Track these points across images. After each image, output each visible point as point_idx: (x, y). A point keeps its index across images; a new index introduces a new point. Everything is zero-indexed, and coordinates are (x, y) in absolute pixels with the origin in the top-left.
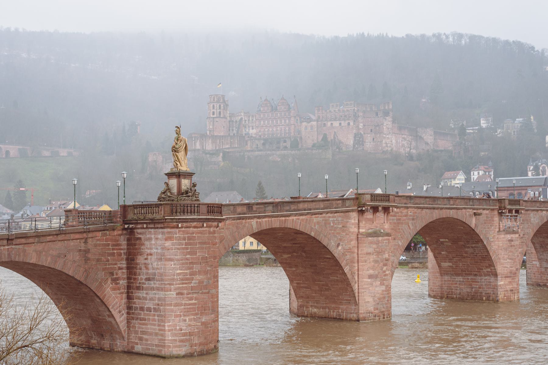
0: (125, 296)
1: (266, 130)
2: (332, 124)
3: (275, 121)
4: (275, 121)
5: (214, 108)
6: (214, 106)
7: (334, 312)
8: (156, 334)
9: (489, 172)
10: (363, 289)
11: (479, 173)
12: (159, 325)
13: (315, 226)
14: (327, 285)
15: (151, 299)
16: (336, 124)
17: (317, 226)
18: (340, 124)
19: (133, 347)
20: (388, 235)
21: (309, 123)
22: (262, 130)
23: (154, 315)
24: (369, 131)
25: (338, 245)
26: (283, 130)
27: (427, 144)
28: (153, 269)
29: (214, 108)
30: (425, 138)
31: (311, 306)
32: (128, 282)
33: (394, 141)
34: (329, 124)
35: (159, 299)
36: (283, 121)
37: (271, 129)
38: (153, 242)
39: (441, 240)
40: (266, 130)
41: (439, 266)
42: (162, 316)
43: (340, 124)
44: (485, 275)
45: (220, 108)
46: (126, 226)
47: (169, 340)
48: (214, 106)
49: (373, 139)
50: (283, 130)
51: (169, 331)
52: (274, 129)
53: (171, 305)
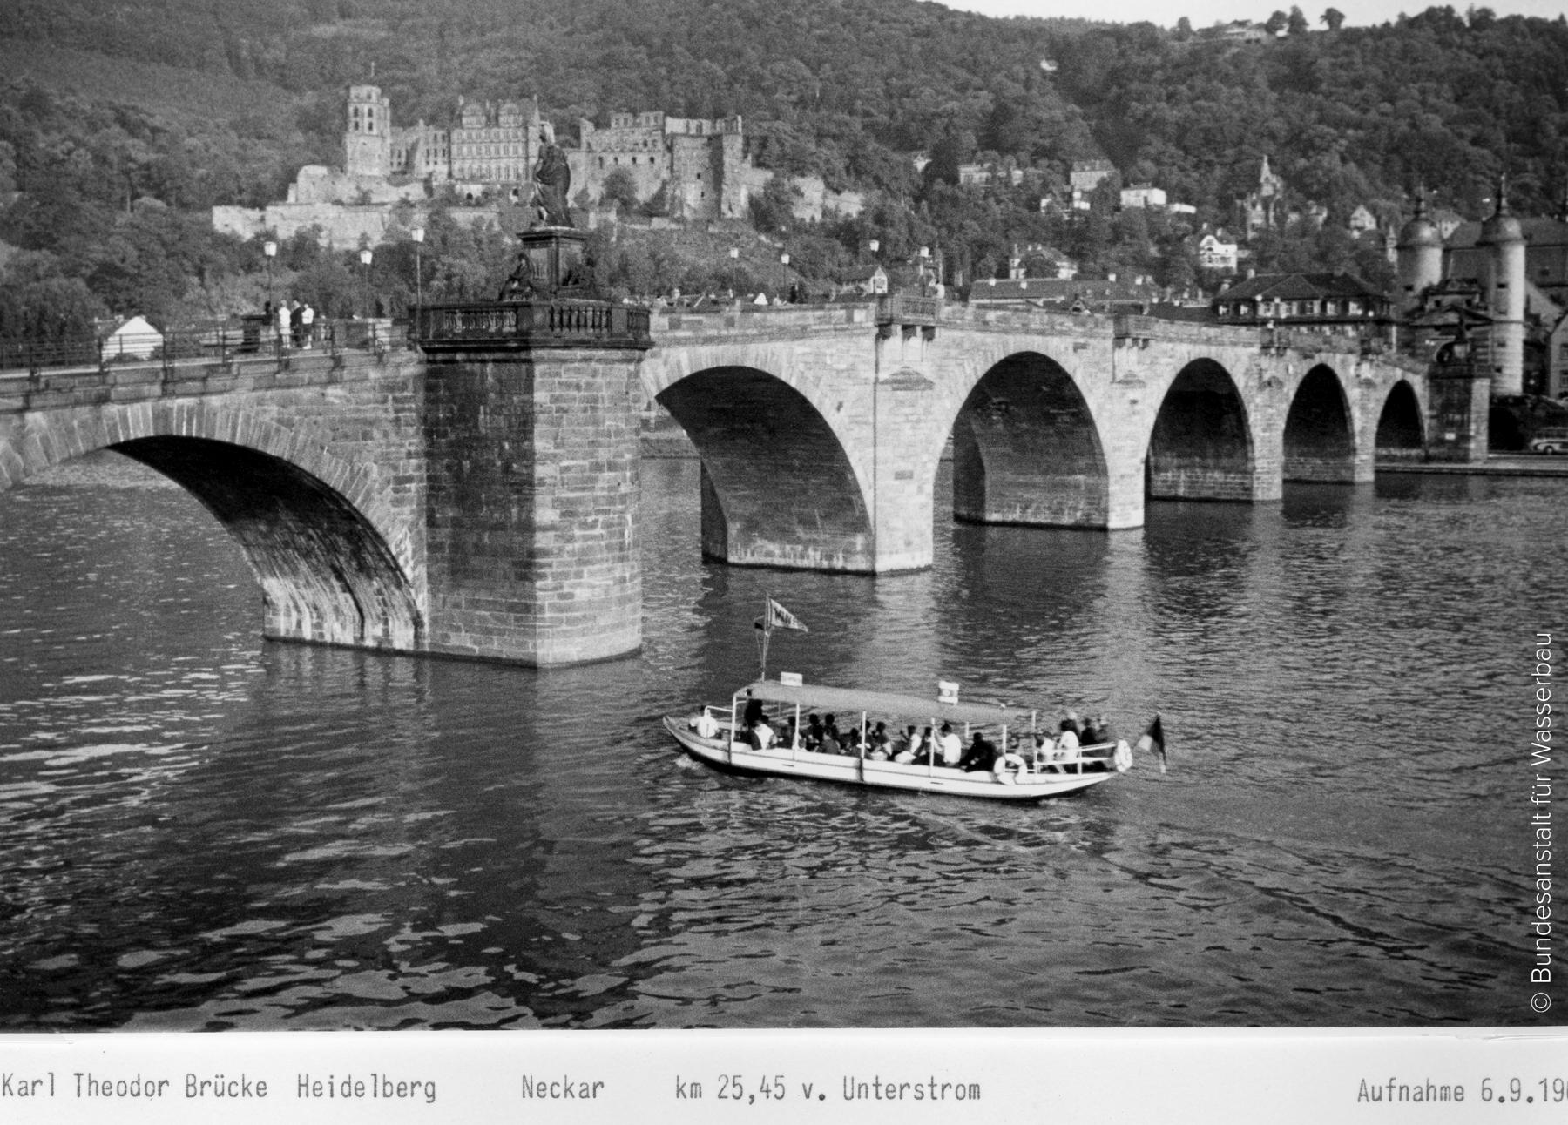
18: (634, 160)
43: (634, 160)
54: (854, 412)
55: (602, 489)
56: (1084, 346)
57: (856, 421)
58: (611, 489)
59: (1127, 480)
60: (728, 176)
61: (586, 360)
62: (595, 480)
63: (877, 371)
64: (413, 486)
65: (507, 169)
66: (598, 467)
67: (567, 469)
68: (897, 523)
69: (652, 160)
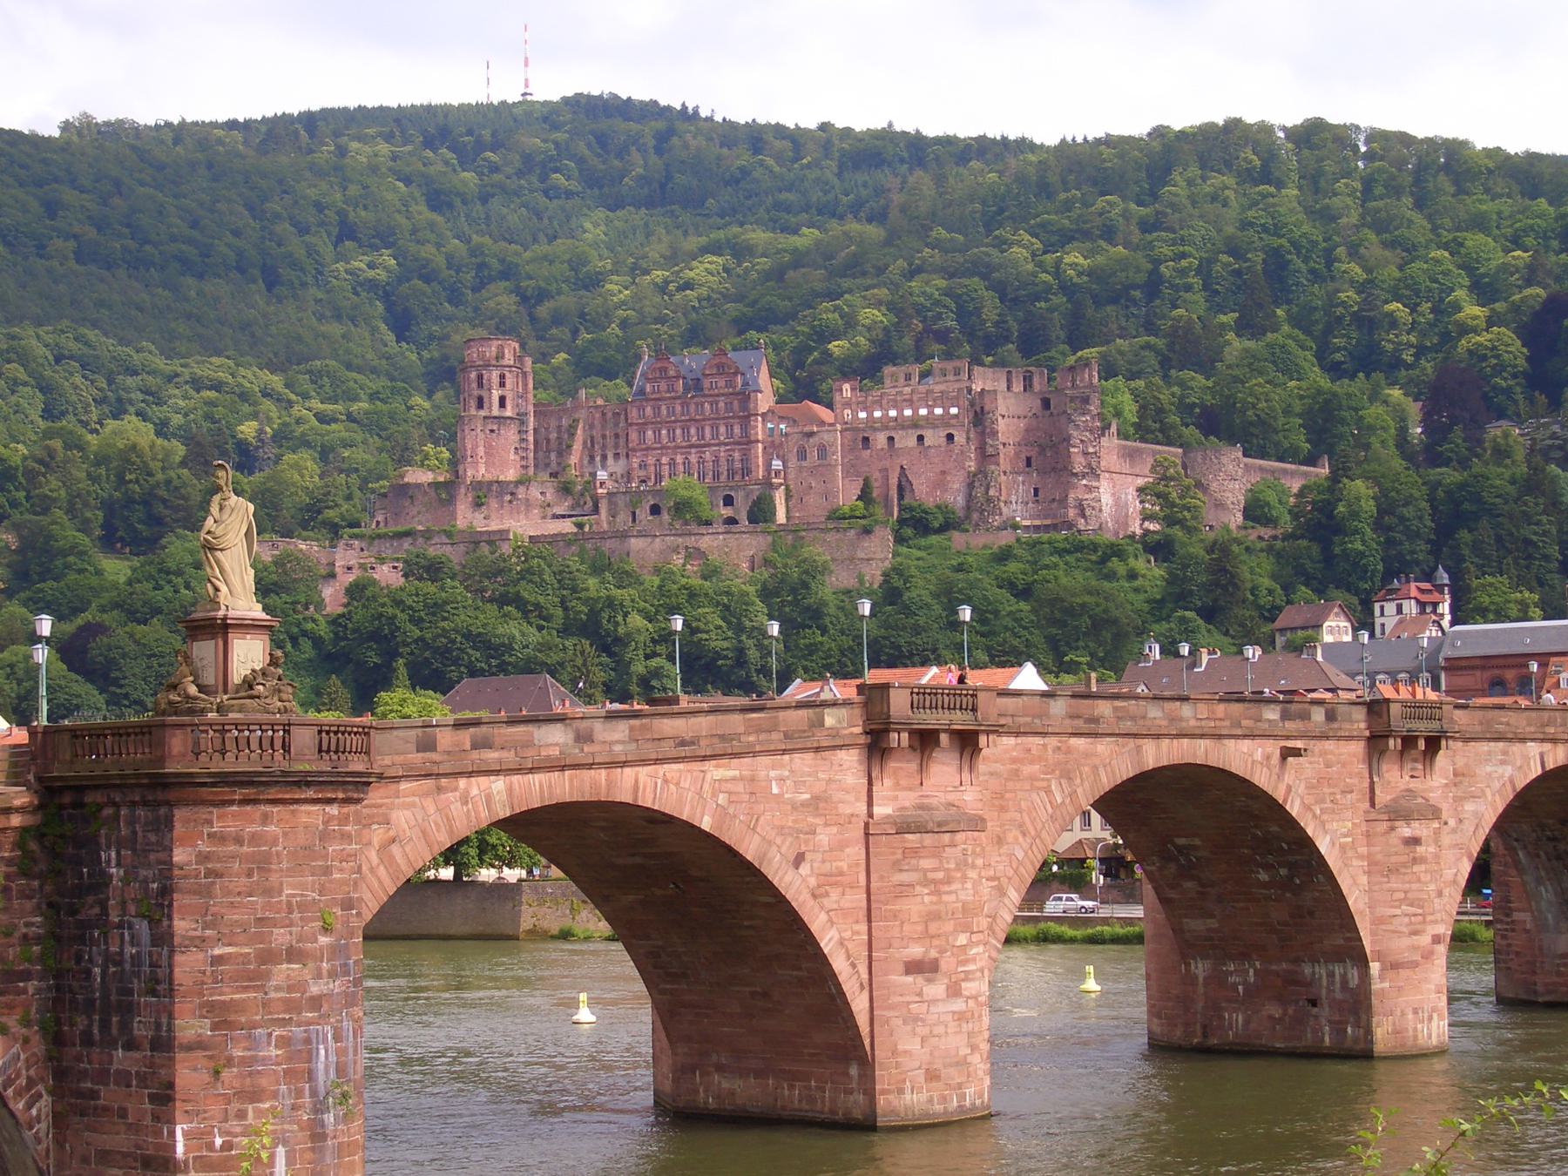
1: (664, 460)
2: (891, 439)
3: (693, 431)
4: (693, 431)
5: (480, 385)
6: (480, 377)
7: (792, 1087)
9: (1435, 605)
10: (891, 1008)
11: (1399, 610)
13: (714, 795)
14: (765, 995)
17: (721, 796)
18: (921, 438)
20: (977, 824)
21: (811, 434)
22: (651, 461)
24: (1022, 464)
25: (799, 860)
26: (723, 462)
27: (1220, 505)
29: (480, 385)
30: (1214, 486)
31: (720, 1068)
33: (1106, 499)
34: (880, 439)
36: (722, 429)
37: (679, 459)
39: (1181, 841)
40: (664, 460)
41: (1178, 931)
43: (921, 438)
45: (502, 385)
48: (480, 377)
49: (1036, 490)
50: (723, 462)
52: (693, 459)
54: (827, 867)
55: (278, 989)
56: (1296, 753)
57: (830, 880)
58: (290, 989)
59: (1404, 973)
60: (1079, 464)
61: (245, 802)
62: (267, 976)
63: (870, 804)
64: (32, 986)
65: (716, 461)
66: (269, 957)
67: (218, 960)
68: (914, 1045)
69: (950, 437)
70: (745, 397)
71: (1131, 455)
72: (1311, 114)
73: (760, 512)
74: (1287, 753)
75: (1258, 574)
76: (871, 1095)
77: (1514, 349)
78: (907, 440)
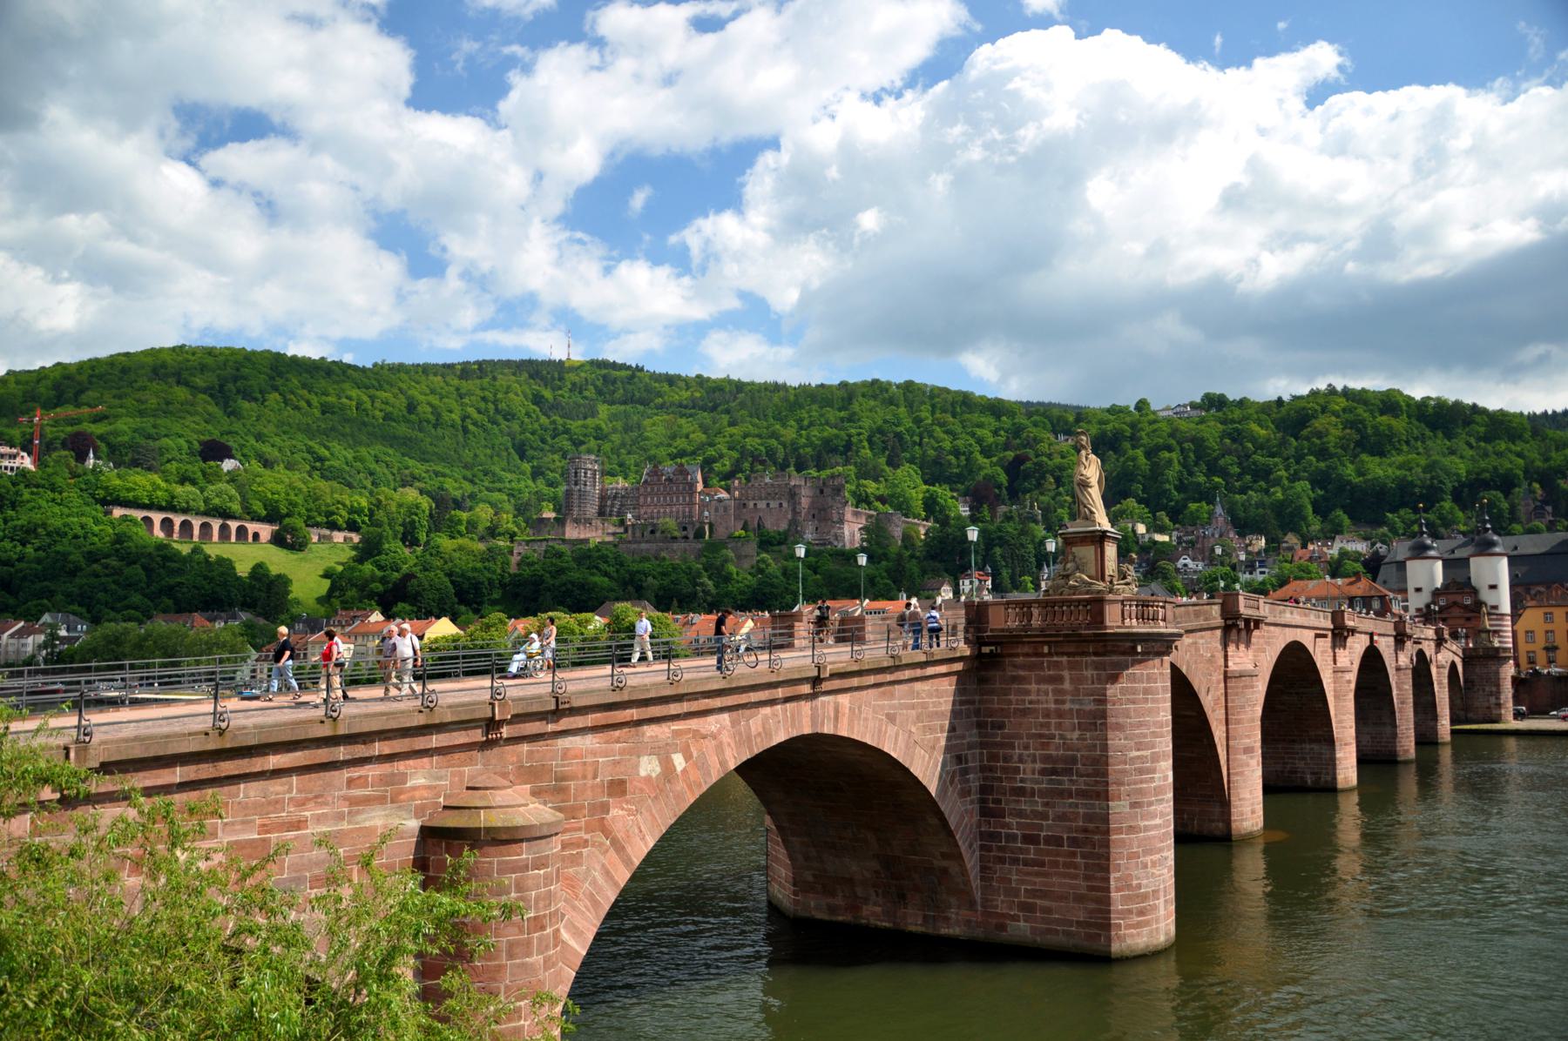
0: (977, 806)
8: (1079, 899)
12: (1087, 878)
15: (1062, 817)
16: (762, 505)
19: (1002, 927)
23: (1074, 854)
28: (1067, 747)
32: (985, 779)
34: (751, 504)
35: (1089, 818)
38: (1067, 685)
42: (1099, 856)
44: (1312, 741)
46: (986, 650)
47: (1118, 912)
51: (1118, 890)
53: (1120, 831)
57: (1216, 701)
70: (692, 485)
71: (856, 514)
72: (908, 378)
73: (699, 534)
74: (1317, 636)
75: (913, 567)
76: (1228, 822)
77: (1003, 478)
78: (762, 505)
